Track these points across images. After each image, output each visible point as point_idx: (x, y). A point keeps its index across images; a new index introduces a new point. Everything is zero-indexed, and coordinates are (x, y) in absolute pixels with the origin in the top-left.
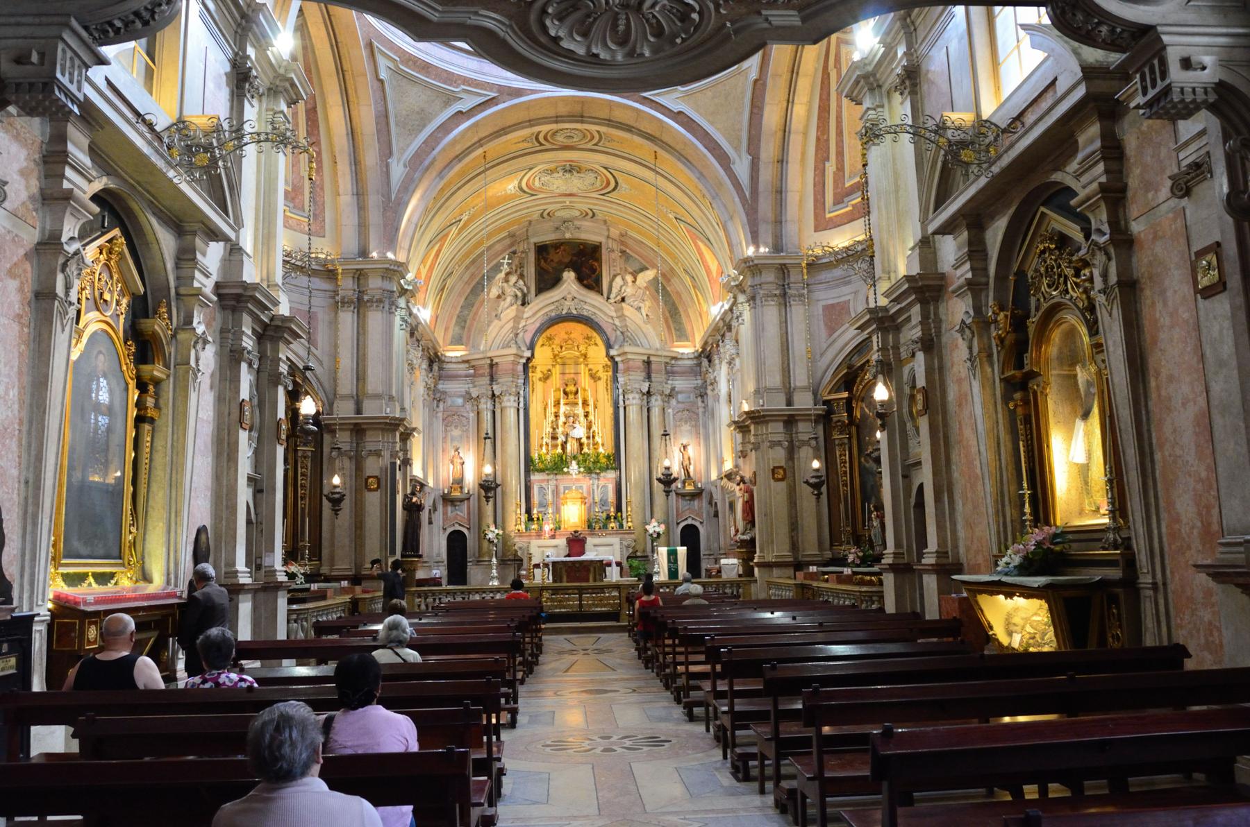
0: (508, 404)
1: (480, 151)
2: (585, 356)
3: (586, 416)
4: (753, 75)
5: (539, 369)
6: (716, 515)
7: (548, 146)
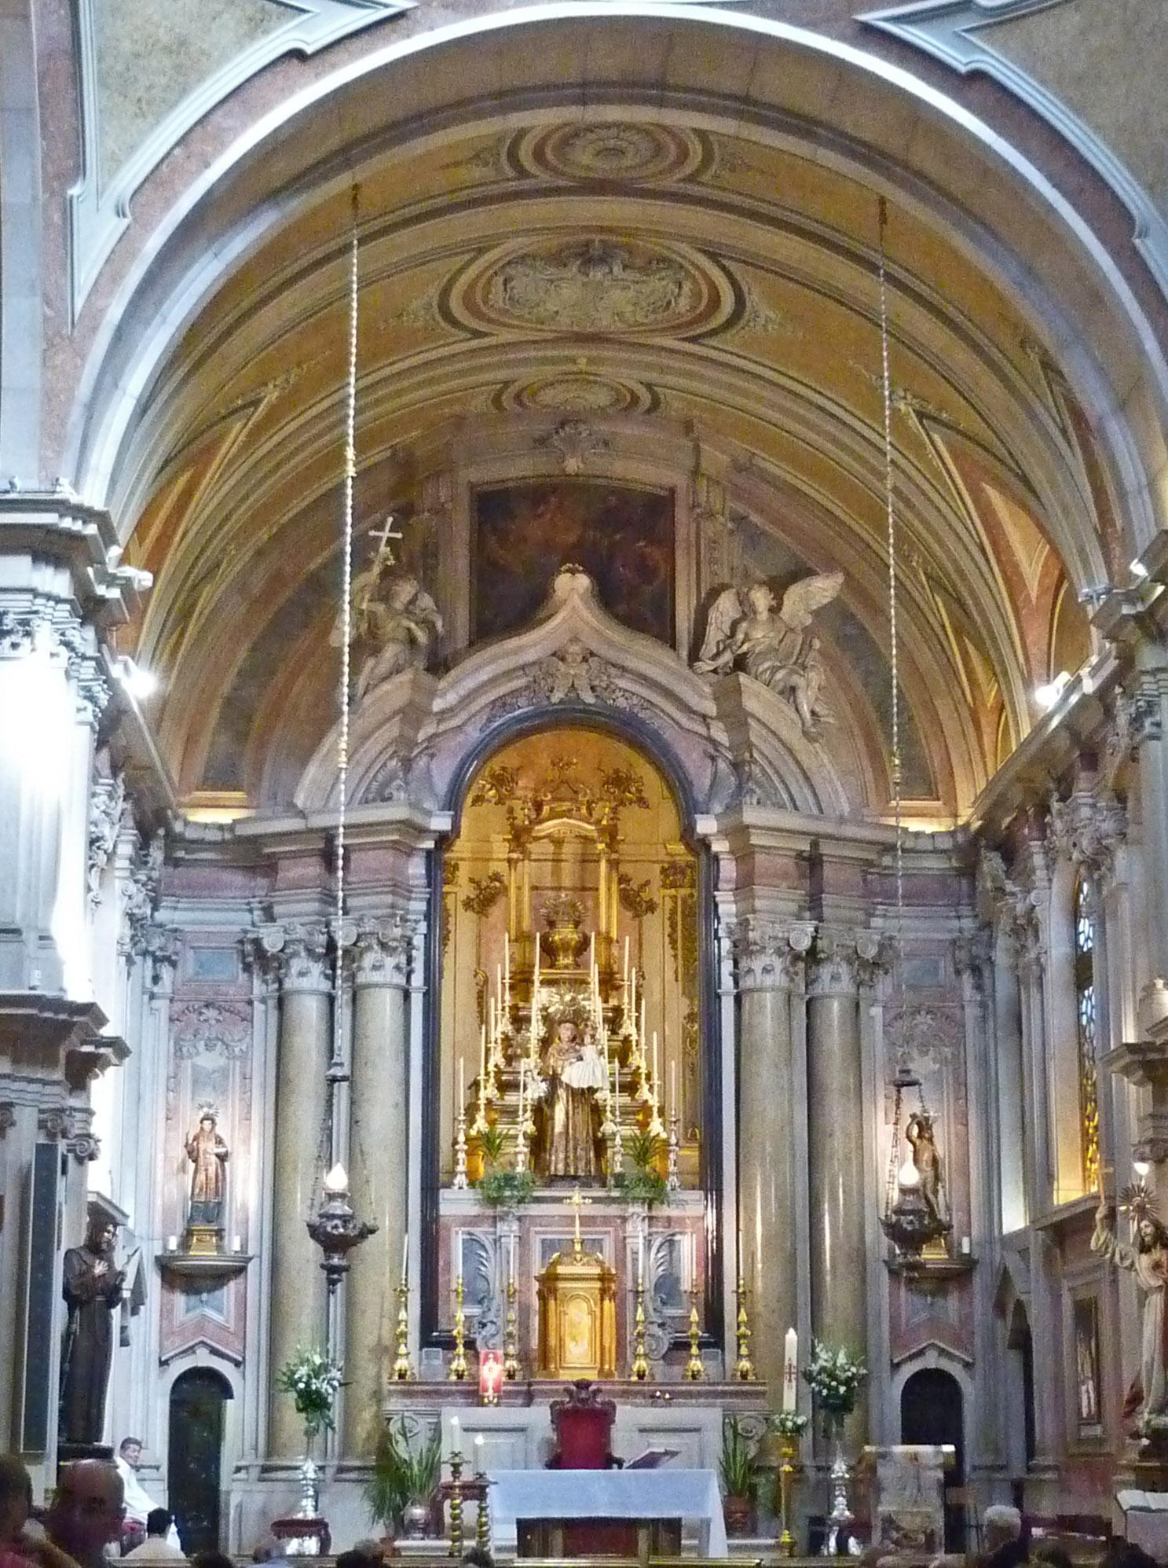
0: (377, 977)
1: (342, 182)
2: (611, 834)
3: (614, 1021)
5: (463, 874)
6: (1022, 1341)
7: (544, 178)
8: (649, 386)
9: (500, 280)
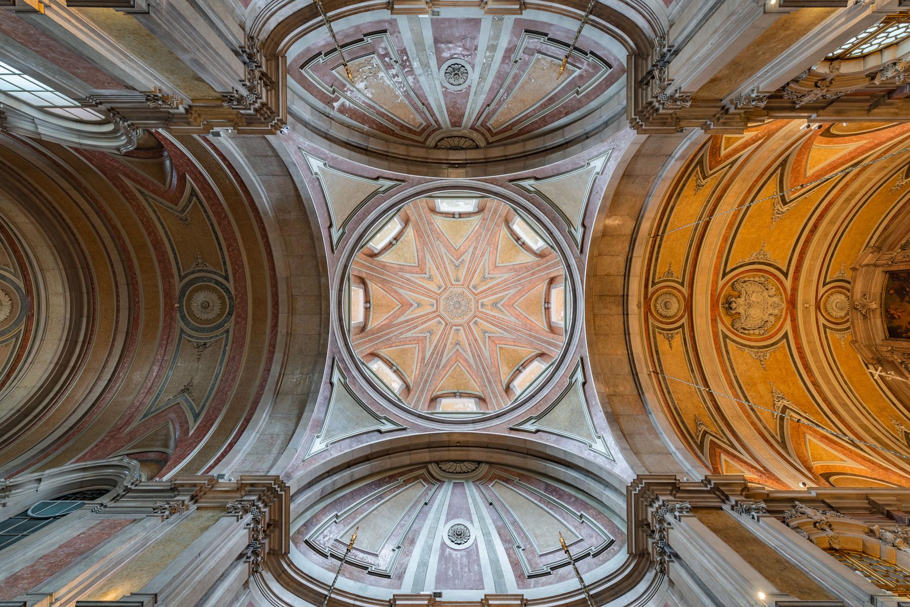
4: (532, 182)
8: (824, 285)
9: (746, 332)
